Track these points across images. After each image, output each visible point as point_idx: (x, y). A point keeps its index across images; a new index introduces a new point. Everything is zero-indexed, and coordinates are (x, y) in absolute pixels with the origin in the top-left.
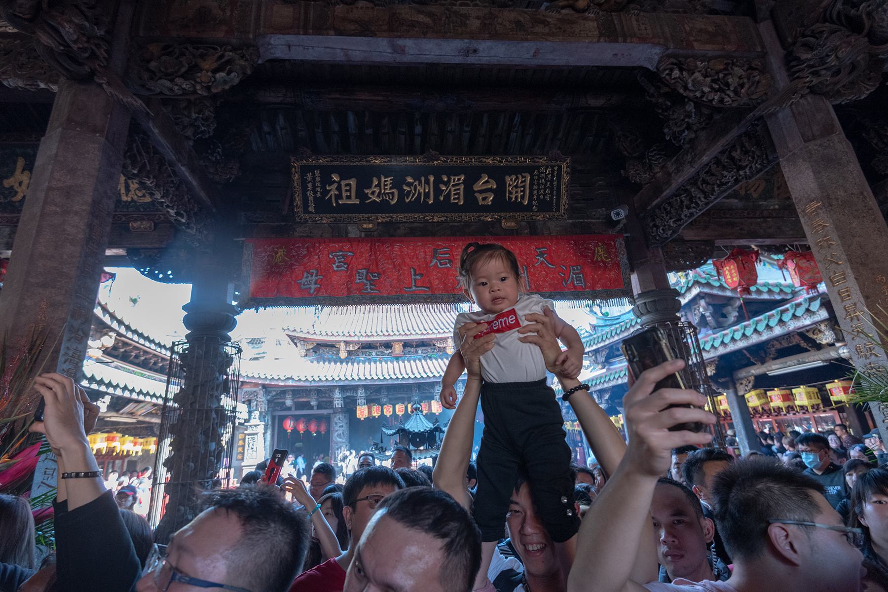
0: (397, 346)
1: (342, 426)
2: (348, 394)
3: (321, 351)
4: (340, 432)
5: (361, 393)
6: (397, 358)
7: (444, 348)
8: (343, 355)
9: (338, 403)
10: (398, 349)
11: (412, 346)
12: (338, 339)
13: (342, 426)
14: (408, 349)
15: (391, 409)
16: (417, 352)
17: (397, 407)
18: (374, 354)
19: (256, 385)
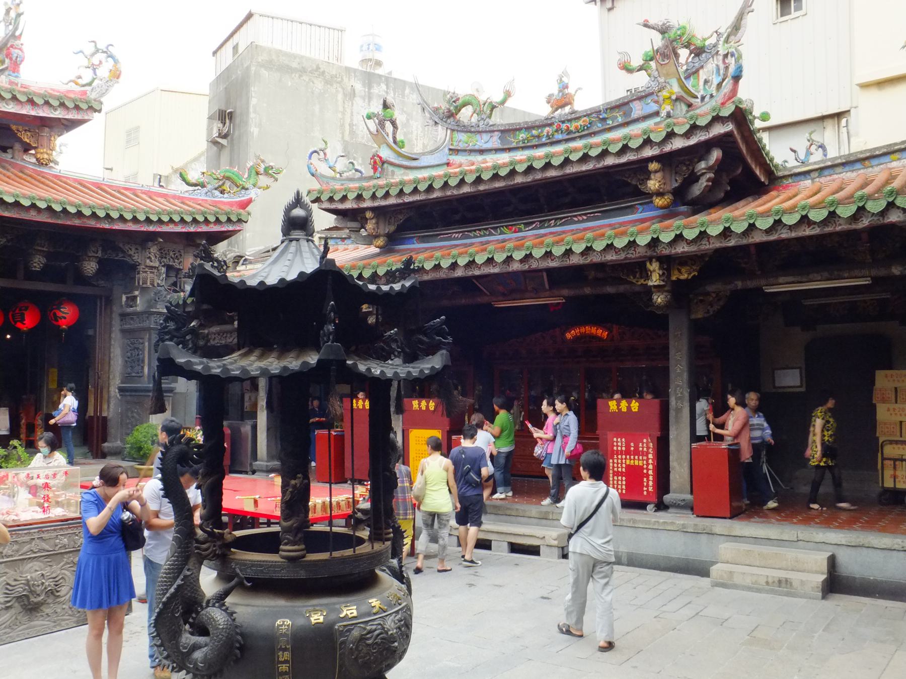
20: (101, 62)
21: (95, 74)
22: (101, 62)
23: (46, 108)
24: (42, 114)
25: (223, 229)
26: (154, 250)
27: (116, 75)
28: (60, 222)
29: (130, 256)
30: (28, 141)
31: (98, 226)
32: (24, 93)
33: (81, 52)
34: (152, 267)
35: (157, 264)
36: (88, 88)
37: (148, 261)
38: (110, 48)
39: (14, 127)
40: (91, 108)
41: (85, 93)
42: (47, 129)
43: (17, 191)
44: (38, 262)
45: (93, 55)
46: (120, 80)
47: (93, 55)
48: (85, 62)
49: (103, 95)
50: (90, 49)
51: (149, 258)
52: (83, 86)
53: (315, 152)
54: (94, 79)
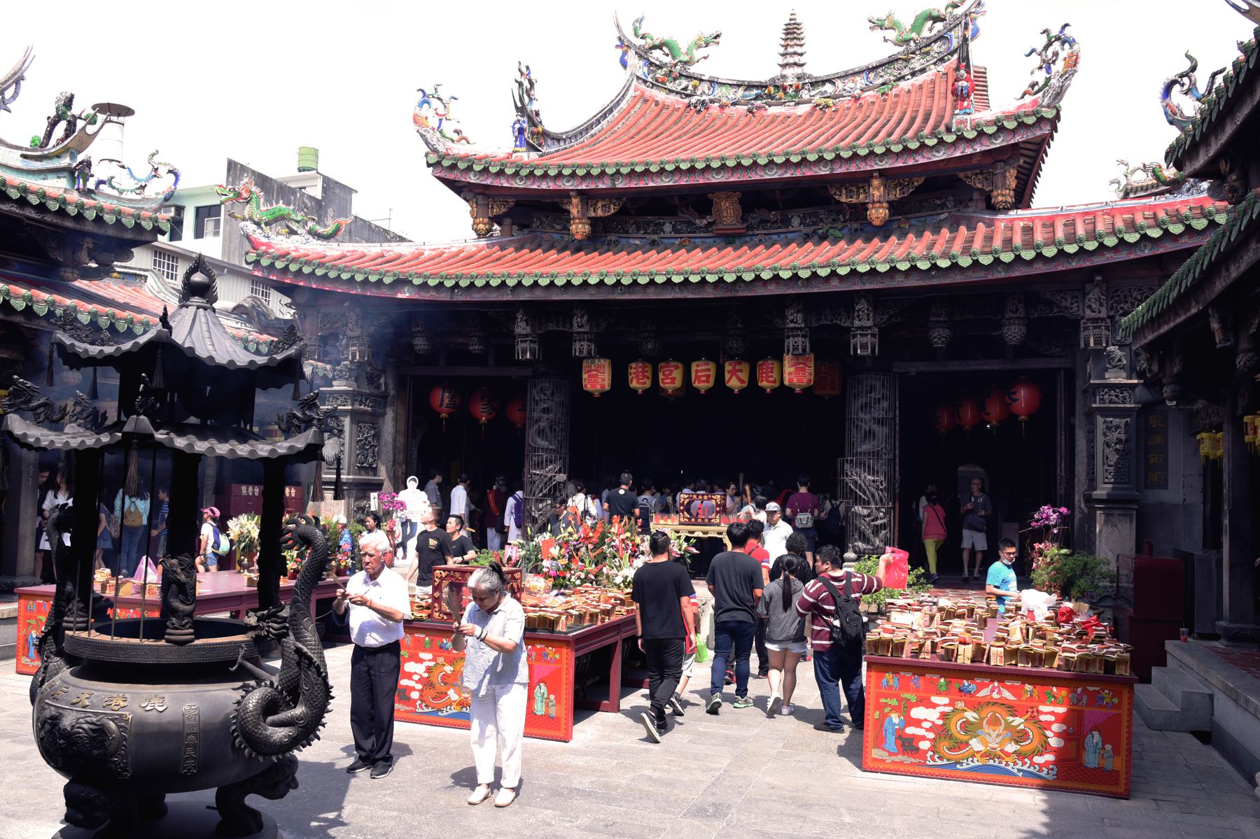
0: (725, 205)
2: (552, 327)
3: (536, 223)
4: (542, 424)
5: (579, 324)
6: (730, 239)
7: (864, 207)
8: (579, 229)
9: (525, 350)
10: (728, 212)
11: (772, 206)
14: (763, 214)
15: (678, 374)
16: (786, 222)
17: (694, 367)
18: (668, 228)
22: (1056, 54)
23: (984, 140)
24: (978, 148)
26: (1094, 294)
27: (1073, 62)
28: (935, 282)
29: (1066, 308)
31: (990, 277)
33: (1033, 51)
34: (1094, 320)
35: (1103, 314)
36: (1040, 94)
37: (1088, 312)
38: (1067, 31)
39: (961, 175)
41: (1035, 101)
43: (706, 265)
44: (939, 337)
45: (1046, 48)
46: (1079, 67)
49: (1059, 94)
51: (1090, 307)
53: (1173, 83)
54: (1048, 80)
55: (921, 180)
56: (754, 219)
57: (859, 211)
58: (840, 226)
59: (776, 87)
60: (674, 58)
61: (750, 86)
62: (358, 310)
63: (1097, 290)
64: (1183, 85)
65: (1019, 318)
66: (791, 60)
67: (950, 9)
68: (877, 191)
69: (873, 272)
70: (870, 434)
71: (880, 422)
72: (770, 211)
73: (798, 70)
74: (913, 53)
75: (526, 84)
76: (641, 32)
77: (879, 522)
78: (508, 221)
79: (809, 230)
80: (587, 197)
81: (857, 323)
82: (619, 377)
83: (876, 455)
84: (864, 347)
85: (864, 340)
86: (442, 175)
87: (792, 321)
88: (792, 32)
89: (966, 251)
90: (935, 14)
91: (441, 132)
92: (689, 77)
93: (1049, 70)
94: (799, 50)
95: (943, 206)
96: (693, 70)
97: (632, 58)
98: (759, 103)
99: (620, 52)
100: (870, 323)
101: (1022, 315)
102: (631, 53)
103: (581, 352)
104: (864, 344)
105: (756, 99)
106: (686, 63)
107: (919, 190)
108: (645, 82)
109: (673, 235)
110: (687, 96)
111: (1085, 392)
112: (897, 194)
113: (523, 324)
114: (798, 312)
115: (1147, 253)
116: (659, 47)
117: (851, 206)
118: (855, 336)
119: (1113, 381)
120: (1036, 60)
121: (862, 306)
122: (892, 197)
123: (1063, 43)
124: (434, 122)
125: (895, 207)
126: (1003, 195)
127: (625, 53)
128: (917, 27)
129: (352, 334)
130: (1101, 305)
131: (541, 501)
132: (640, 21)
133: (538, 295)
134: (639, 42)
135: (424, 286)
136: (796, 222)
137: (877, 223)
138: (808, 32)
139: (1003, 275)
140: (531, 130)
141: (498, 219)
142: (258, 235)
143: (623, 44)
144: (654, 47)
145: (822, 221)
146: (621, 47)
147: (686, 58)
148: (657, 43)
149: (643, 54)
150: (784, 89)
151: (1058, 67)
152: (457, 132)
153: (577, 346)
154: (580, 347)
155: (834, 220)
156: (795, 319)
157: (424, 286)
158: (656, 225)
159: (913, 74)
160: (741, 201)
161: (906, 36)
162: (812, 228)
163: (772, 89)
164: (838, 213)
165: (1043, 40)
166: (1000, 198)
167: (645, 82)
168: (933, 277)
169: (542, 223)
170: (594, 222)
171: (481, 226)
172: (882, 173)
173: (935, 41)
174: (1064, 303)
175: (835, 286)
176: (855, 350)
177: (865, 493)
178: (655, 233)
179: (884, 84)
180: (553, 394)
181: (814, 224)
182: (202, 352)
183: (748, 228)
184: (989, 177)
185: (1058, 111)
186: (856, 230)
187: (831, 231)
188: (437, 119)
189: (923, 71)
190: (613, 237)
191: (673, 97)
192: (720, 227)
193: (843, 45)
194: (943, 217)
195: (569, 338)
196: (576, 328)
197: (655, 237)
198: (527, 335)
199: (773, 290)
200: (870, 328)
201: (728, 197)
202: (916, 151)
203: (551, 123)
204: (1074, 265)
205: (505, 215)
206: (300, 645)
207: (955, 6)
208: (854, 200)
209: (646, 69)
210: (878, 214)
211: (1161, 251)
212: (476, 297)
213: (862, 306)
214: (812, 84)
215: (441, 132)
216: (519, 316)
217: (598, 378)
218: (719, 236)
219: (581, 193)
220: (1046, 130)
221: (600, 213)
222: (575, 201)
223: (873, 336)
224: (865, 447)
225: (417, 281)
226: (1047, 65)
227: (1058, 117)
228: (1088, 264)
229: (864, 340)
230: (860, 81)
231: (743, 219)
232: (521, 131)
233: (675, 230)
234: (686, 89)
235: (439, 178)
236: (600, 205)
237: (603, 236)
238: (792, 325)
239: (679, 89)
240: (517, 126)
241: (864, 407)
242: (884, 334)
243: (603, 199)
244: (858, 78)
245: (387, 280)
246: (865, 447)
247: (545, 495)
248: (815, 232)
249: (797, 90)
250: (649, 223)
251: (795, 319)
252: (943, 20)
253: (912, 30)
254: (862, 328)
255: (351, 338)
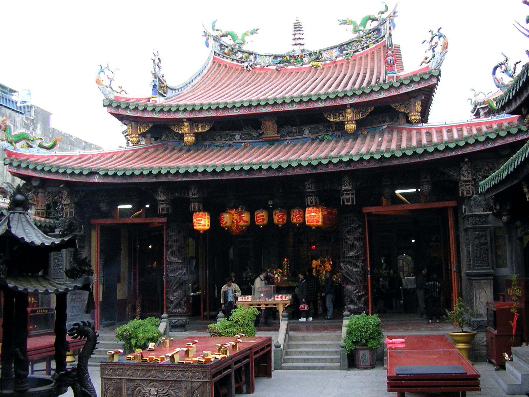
1: (176, 241)
4: (174, 249)
5: (193, 194)
6: (271, 142)
7: (343, 124)
8: (189, 139)
11: (293, 124)
12: (180, 116)
13: (176, 241)
16: (301, 132)
18: (237, 137)
19: (58, 182)
20: (437, 43)
21: (434, 51)
22: (437, 43)
25: (518, 139)
26: (465, 168)
27: (445, 47)
29: (452, 175)
30: (403, 111)
32: (406, 79)
35: (470, 179)
36: (430, 63)
39: (393, 105)
40: (432, 76)
41: (428, 67)
42: (412, 100)
46: (448, 49)
47: (433, 38)
48: (429, 47)
49: (440, 65)
50: (429, 36)
52: (428, 62)
54: (434, 56)
55: (372, 108)
56: (285, 131)
57: (341, 126)
58: (330, 134)
59: (290, 56)
60: (234, 41)
61: (276, 57)
62: (68, 189)
63: (466, 165)
64: (501, 68)
65: (427, 181)
66: (297, 42)
67: (380, 15)
68: (349, 115)
69: (351, 161)
70: (353, 246)
71: (357, 239)
72: (293, 126)
73: (302, 47)
74: (362, 37)
75: (157, 61)
76: (216, 28)
77: (360, 294)
78: (149, 136)
79: (313, 136)
80: (193, 121)
81: (344, 188)
82: (215, 221)
83: (357, 257)
84: (348, 200)
85: (348, 197)
86: (114, 111)
87: (309, 188)
88: (297, 27)
89: (399, 147)
90: (372, 17)
91: (111, 88)
92: (243, 52)
93: (434, 51)
94: (301, 36)
95: (384, 122)
96: (244, 48)
97: (211, 42)
98: (281, 65)
99: (205, 39)
100: (350, 188)
101: (429, 180)
102: (211, 39)
103: (195, 209)
104: (348, 197)
105: (279, 63)
106: (241, 44)
107: (371, 114)
108: (219, 55)
109: (240, 141)
110: (242, 62)
111: (463, 218)
112: (360, 117)
113: (162, 195)
114: (312, 183)
115: (489, 146)
116: (226, 36)
117: (336, 123)
118: (343, 195)
119: (477, 213)
120: (427, 46)
121: (346, 178)
122: (357, 118)
123: (440, 37)
124: (106, 82)
125: (358, 122)
126: (415, 116)
127: (208, 39)
128: (364, 24)
129: (65, 203)
130: (469, 173)
131: (175, 291)
132: (214, 22)
133: (170, 179)
134: (215, 34)
135: (106, 175)
136: (307, 132)
137: (350, 132)
138: (304, 26)
139: (418, 160)
140: (160, 87)
141: (143, 135)
142: (10, 148)
143: (205, 34)
144: (223, 36)
145: (320, 131)
146: (205, 36)
147: (240, 42)
148: (225, 34)
149: (216, 39)
150: (295, 57)
151: (438, 49)
152: (120, 87)
153: (192, 205)
154: (193, 205)
155: (327, 131)
156: (310, 187)
157: (106, 175)
158: (231, 136)
159: (363, 49)
160: (277, 122)
161: (357, 29)
162: (316, 135)
163: (288, 57)
164: (329, 127)
165: (430, 36)
166: (413, 117)
167: (219, 55)
168: (383, 162)
169: (167, 136)
170: (197, 135)
171: (134, 139)
172: (352, 105)
173: (373, 31)
174: (452, 173)
175: (332, 169)
176: (343, 202)
177: (352, 278)
178: (230, 140)
179: (348, 54)
180: (179, 232)
181: (317, 133)
182: (27, 240)
183: (281, 136)
184: (408, 106)
185: (440, 72)
186: (339, 136)
187: (326, 137)
188: (109, 81)
189: (368, 47)
190: (207, 143)
191: (234, 62)
192: (266, 136)
193: (325, 35)
194: (384, 127)
195: (188, 201)
196: (191, 196)
197: (230, 142)
198: (163, 201)
199: (298, 172)
200: (350, 190)
201: (270, 120)
202: (369, 94)
203: (170, 82)
204: (454, 153)
205: (147, 132)
206: (83, 389)
207: (383, 13)
208: (337, 120)
209: (219, 48)
210: (351, 127)
211: (497, 145)
212: (136, 180)
213: (346, 178)
214: (309, 54)
215: (111, 88)
216: (160, 190)
217: (202, 222)
218: (266, 141)
219: (189, 120)
220: (434, 81)
221: (200, 130)
222: (186, 124)
223: (352, 194)
224: (351, 254)
225: (102, 173)
226: (433, 48)
227: (440, 74)
228: (461, 153)
229: (348, 197)
230: (335, 53)
231: (278, 132)
232: (155, 86)
233: (241, 138)
234: (242, 58)
235: (110, 113)
236: (200, 126)
237: (202, 142)
238: (309, 190)
239: (238, 58)
240: (153, 84)
241: (349, 232)
242: (358, 193)
243: (202, 122)
244: (334, 51)
245: (85, 173)
246: (351, 254)
247: (177, 288)
248: (317, 137)
249: (302, 57)
250: (227, 135)
251: (310, 187)
252: (377, 20)
253: (361, 25)
254: (346, 190)
255: (65, 205)
